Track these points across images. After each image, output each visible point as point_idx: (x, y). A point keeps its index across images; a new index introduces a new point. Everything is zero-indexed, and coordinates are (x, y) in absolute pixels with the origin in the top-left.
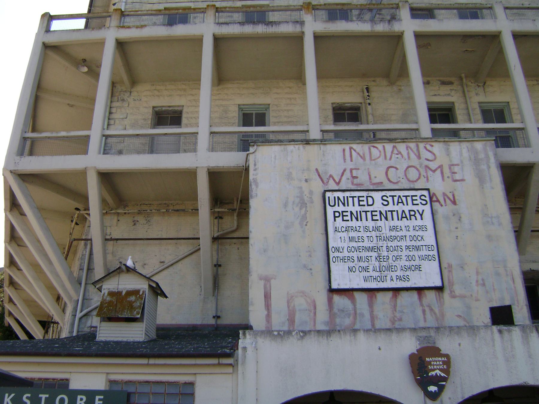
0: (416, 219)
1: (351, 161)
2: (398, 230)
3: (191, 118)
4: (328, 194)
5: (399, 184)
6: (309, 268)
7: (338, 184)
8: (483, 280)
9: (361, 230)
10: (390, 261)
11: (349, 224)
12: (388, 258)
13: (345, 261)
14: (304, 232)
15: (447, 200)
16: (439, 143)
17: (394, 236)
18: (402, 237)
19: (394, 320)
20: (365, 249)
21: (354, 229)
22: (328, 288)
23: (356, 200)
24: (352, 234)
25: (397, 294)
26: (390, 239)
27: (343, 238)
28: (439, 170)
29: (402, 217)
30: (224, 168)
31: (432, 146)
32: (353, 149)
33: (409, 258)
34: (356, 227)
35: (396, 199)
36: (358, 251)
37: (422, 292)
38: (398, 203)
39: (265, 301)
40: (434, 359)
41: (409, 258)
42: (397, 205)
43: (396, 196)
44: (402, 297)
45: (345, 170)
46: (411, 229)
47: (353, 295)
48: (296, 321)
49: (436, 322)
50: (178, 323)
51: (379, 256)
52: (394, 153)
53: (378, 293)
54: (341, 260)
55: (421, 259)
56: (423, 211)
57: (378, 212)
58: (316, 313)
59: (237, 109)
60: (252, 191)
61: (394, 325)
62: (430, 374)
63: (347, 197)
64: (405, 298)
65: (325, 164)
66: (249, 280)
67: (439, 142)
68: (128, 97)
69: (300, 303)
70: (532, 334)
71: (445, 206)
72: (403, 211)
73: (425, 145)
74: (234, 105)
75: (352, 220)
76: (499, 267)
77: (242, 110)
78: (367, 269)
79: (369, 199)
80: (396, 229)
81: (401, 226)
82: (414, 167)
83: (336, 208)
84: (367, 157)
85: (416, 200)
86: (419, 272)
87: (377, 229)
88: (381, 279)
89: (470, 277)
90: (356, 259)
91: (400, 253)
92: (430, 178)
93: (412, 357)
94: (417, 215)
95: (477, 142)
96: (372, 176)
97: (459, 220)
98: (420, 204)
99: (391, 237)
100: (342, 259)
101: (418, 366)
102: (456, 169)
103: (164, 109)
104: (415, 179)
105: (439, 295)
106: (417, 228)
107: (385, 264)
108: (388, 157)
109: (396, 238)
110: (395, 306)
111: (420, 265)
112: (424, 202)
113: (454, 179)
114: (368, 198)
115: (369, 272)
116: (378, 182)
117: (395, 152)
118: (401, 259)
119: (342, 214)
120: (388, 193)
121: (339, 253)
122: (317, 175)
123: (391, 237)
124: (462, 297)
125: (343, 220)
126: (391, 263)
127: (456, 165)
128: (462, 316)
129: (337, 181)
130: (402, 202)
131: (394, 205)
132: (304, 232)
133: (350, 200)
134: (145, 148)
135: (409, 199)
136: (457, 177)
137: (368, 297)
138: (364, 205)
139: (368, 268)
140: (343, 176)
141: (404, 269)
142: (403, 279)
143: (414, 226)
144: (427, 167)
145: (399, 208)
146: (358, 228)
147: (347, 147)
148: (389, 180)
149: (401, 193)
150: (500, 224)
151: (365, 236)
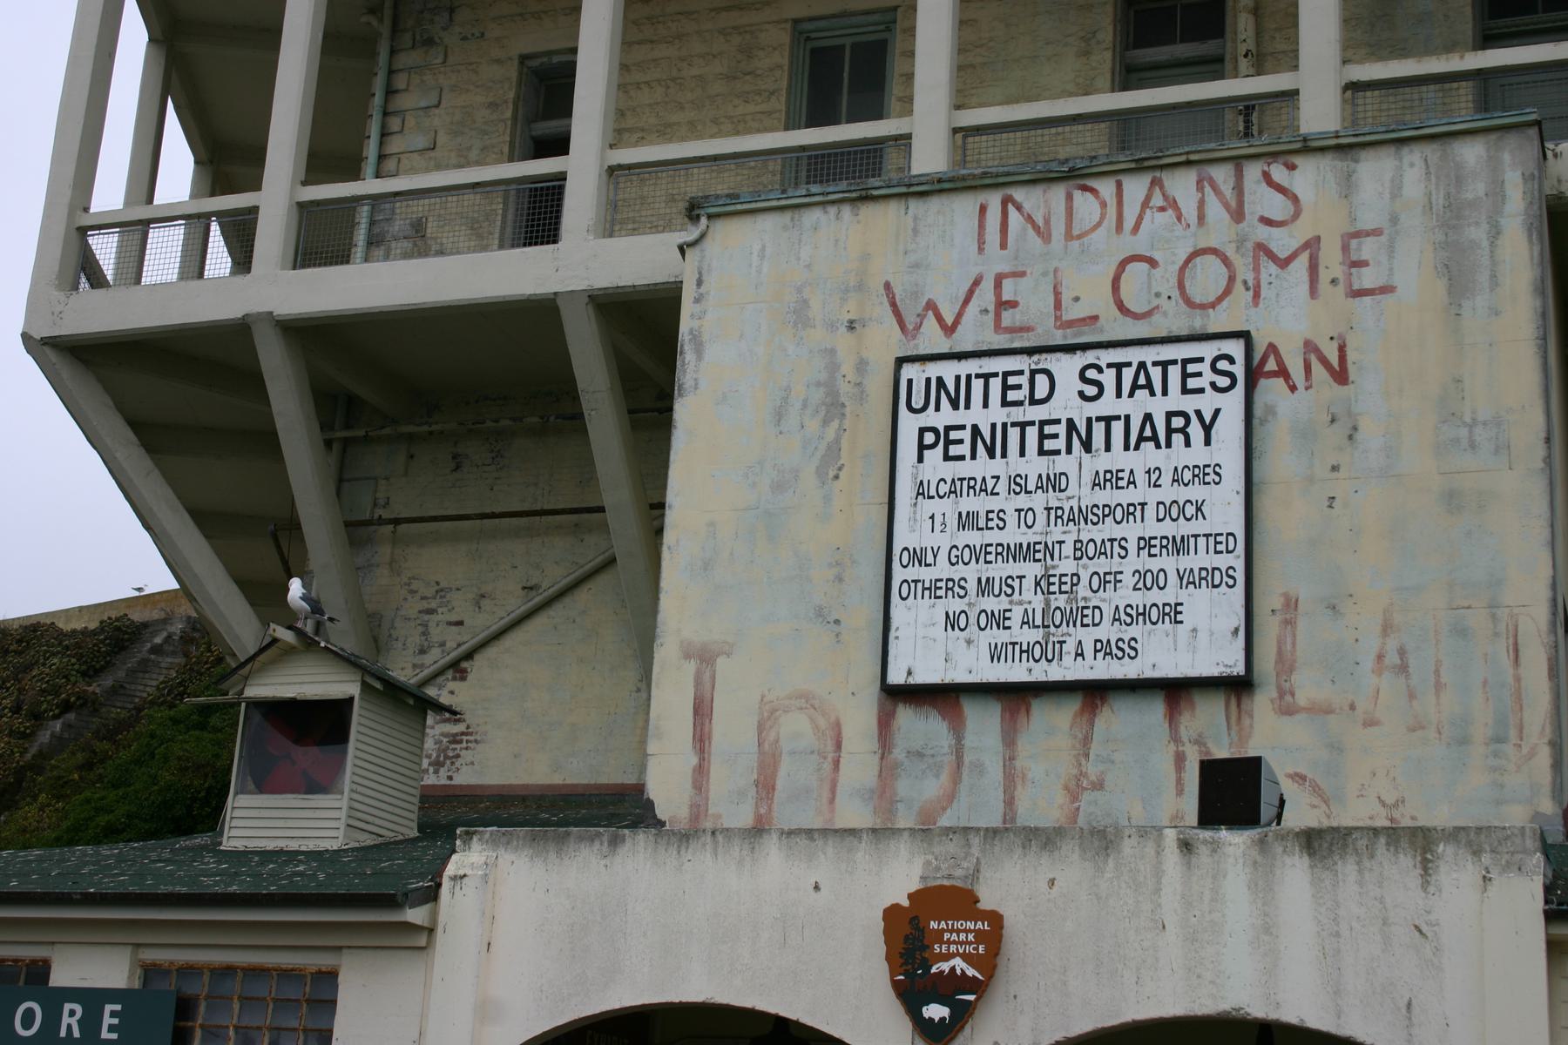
0: (1188, 444)
1: (1003, 246)
2: (1121, 483)
3: (638, 86)
5: (1156, 318)
6: (831, 619)
7: (949, 330)
8: (1402, 652)
9: (1002, 487)
10: (1082, 590)
11: (965, 469)
13: (939, 593)
14: (827, 499)
15: (1317, 367)
16: (1319, 155)
17: (1104, 506)
19: (1078, 785)
20: (1005, 554)
21: (978, 488)
24: (969, 503)
25: (1099, 703)
26: (1090, 517)
27: (939, 519)
28: (1304, 259)
29: (1141, 439)
30: (637, 289)
31: (1292, 167)
34: (984, 479)
35: (1128, 374)
38: (1135, 387)
40: (953, 925)
42: (1131, 395)
43: (1129, 364)
44: (1112, 711)
45: (977, 283)
46: (1166, 479)
48: (779, 784)
50: (569, 781)
53: (1036, 696)
54: (927, 593)
56: (1217, 412)
57: (1064, 422)
58: (838, 761)
59: (785, 38)
60: (685, 371)
62: (934, 970)
63: (969, 377)
64: (1118, 719)
65: (917, 265)
66: (655, 661)
68: (444, 29)
69: (796, 728)
70: (1288, 860)
71: (1307, 389)
72: (1148, 417)
74: (778, 22)
75: (973, 457)
77: (808, 39)
78: (1005, 619)
80: (1114, 480)
81: (1132, 471)
83: (931, 418)
85: (1199, 374)
87: (1053, 483)
88: (1044, 652)
89: (1357, 640)
90: (972, 586)
92: (1264, 293)
93: (892, 913)
94: (1196, 430)
97: (1350, 437)
98: (1208, 389)
99: (1095, 510)
100: (930, 589)
101: (905, 943)
102: (1367, 249)
103: (556, 59)
104: (1212, 299)
105: (1239, 705)
106: (1188, 475)
107: (1060, 601)
108: (1129, 223)
109: (1112, 512)
110: (1087, 741)
111: (1181, 604)
112: (1223, 382)
113: (1356, 287)
115: (1009, 628)
116: (1082, 315)
117: (1158, 200)
118: (1118, 585)
119: (945, 437)
120: (1106, 357)
122: (886, 304)
123: (1095, 510)
124: (1321, 710)
125: (947, 458)
126: (1085, 599)
127: (1368, 234)
128: (1310, 776)
129: (949, 321)
130: (1149, 386)
131: (1119, 395)
132: (827, 499)
133: (978, 385)
134: (494, 207)
135: (1174, 373)
136: (1367, 278)
138: (1019, 403)
139: (1007, 614)
141: (1123, 617)
142: (1115, 651)
143: (1176, 469)
144: (1262, 249)
146: (990, 483)
147: (994, 200)
148: (1121, 307)
149: (1149, 354)
150: (1502, 448)
151: (1010, 510)
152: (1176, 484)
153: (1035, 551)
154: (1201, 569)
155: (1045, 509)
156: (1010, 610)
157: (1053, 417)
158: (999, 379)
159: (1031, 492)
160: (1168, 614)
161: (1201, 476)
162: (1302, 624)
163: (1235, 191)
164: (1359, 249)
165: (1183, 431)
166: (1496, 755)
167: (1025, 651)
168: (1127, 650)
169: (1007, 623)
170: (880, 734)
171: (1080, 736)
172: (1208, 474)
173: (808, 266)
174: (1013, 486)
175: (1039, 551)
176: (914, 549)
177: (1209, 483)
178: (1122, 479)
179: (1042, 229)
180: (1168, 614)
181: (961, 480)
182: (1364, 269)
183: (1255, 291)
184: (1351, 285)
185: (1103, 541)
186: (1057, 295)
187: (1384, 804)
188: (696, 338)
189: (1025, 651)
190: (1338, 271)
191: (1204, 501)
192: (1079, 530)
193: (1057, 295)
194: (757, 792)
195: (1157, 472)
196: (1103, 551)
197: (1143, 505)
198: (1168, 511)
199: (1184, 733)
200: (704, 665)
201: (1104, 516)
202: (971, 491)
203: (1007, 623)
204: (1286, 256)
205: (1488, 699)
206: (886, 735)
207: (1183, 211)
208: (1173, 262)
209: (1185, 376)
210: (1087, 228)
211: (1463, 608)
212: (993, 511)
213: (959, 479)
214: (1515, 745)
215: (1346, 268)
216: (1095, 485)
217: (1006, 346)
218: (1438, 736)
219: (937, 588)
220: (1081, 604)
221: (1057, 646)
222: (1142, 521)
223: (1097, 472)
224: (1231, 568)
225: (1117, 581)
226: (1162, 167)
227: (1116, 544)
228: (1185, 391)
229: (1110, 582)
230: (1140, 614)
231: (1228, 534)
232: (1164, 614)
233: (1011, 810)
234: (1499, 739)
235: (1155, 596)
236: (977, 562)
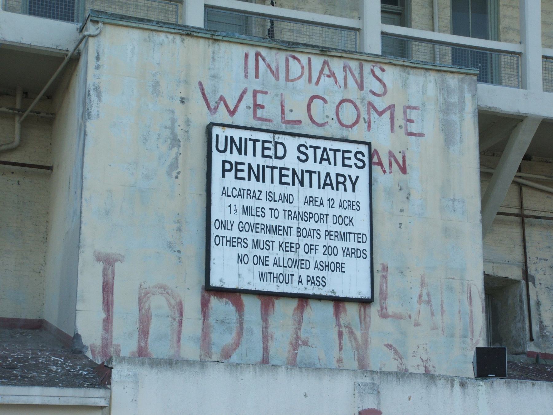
0: (345, 190)
1: (257, 76)
2: (317, 203)
4: (216, 131)
5: (327, 127)
6: (176, 249)
7: (232, 113)
8: (428, 295)
9: (263, 196)
10: (301, 251)
11: (245, 184)
12: (298, 247)
13: (234, 244)
15: (394, 164)
16: (394, 67)
17: (310, 213)
18: (322, 216)
19: (297, 343)
21: (252, 195)
23: (259, 145)
25: (305, 304)
26: (304, 217)
27: (233, 208)
28: (388, 114)
29: (325, 184)
30: (32, 47)
31: (383, 70)
32: (261, 56)
33: (330, 251)
34: (254, 191)
35: (319, 152)
37: (341, 304)
38: (322, 159)
39: (103, 296)
41: (330, 251)
42: (321, 162)
43: (319, 148)
45: (244, 92)
46: (337, 205)
47: (240, 300)
48: (151, 331)
49: (356, 352)
51: (286, 243)
52: (324, 73)
53: (277, 299)
54: (228, 243)
56: (358, 177)
58: (181, 322)
61: (296, 352)
63: (246, 139)
65: (214, 77)
67: (395, 65)
71: (390, 173)
72: (328, 175)
73: (374, 67)
76: (453, 279)
78: (266, 261)
79: (280, 147)
80: (314, 201)
81: (322, 199)
82: (351, 102)
84: (282, 75)
85: (350, 158)
86: (341, 273)
87: (287, 198)
88: (284, 278)
89: (411, 288)
90: (250, 243)
91: (315, 241)
94: (348, 184)
95: (451, 75)
97: (408, 198)
98: (354, 166)
99: (306, 214)
100: (230, 241)
102: (413, 115)
104: (350, 123)
105: (365, 312)
106: (346, 205)
108: (314, 79)
110: (300, 322)
111: (344, 264)
112: (360, 164)
113: (409, 131)
115: (268, 265)
117: (326, 71)
118: (317, 251)
119: (236, 167)
123: (306, 214)
124: (398, 317)
125: (236, 178)
126: (302, 255)
127: (413, 108)
128: (394, 346)
129: (232, 108)
130: (328, 159)
131: (315, 162)
135: (339, 155)
136: (413, 128)
137: (262, 304)
138: (270, 157)
139: (267, 259)
141: (319, 266)
142: (316, 282)
144: (370, 104)
145: (323, 168)
146: (258, 194)
147: (252, 52)
151: (267, 209)
152: (341, 208)
153: (279, 230)
154: (352, 249)
155: (283, 210)
156: (268, 257)
157: (286, 166)
159: (276, 201)
160: (338, 267)
162: (390, 278)
163: (360, 75)
164: (410, 114)
165: (343, 183)
166: (464, 342)
167: (275, 277)
168: (321, 282)
169: (267, 263)
170: (203, 310)
171: (297, 319)
172: (354, 205)
173: (159, 64)
175: (281, 230)
177: (355, 210)
178: (317, 201)
179: (275, 73)
180: (338, 267)
181: (244, 190)
183: (368, 124)
184: (407, 130)
185: (310, 230)
186: (282, 106)
187: (422, 360)
188: (97, 89)
191: (353, 217)
192: (299, 223)
193: (282, 106)
194: (139, 334)
195: (333, 200)
197: (327, 215)
198: (338, 220)
199: (342, 322)
200: (108, 266)
201: (310, 218)
202: (249, 196)
203: (267, 263)
204: (381, 111)
205: (461, 319)
206: (205, 311)
207: (337, 79)
208: (334, 103)
209: (344, 158)
210: (295, 77)
211: (451, 279)
212: (259, 208)
213: (242, 189)
214: (471, 339)
215: (405, 121)
216: (305, 202)
217: (259, 127)
218: (442, 333)
219: (233, 242)
220: (301, 258)
221: (290, 277)
222: (327, 223)
223: (306, 197)
225: (316, 249)
226: (328, 56)
227: (315, 232)
228: (344, 165)
229: (313, 249)
230: (327, 266)
232: (337, 267)
233: (267, 352)
234: (465, 336)
235: (332, 258)
236: (252, 231)
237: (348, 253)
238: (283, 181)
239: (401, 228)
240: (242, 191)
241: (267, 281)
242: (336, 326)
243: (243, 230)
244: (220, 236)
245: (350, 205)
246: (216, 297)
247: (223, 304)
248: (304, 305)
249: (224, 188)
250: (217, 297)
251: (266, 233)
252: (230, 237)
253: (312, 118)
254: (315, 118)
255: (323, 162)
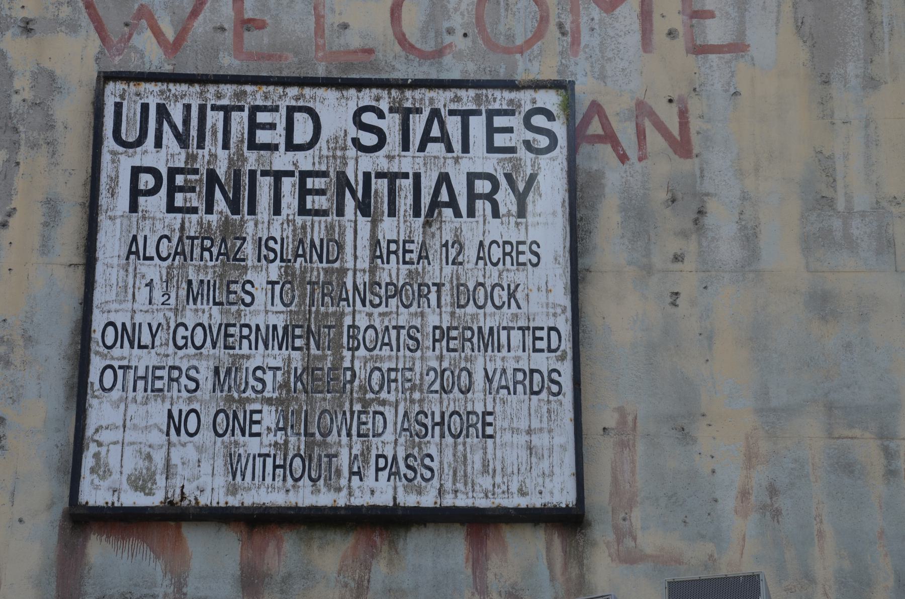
0: (496, 214)
5: (448, 59)
13: (159, 384)
21: (215, 251)
22: (65, 503)
35: (418, 125)
36: (221, 343)
38: (426, 139)
42: (422, 148)
43: (419, 111)
54: (141, 384)
55: (495, 385)
63: (202, 109)
71: (640, 159)
72: (444, 179)
78: (253, 422)
83: (148, 156)
85: (510, 130)
89: (713, 472)
92: (585, 38)
94: (506, 199)
96: (332, 20)
100: (145, 378)
104: (519, 41)
106: (496, 253)
111: (490, 414)
114: (297, 115)
115: (258, 435)
121: (136, 351)
125: (171, 208)
129: (170, 34)
130: (445, 138)
131: (406, 147)
135: (477, 125)
139: (256, 417)
140: (201, 18)
142: (403, 469)
148: (402, 40)
156: (260, 412)
158: (245, 114)
161: (514, 254)
165: (490, 197)
167: (279, 467)
169: (256, 428)
172: (523, 253)
174: (264, 251)
176: (124, 325)
177: (524, 264)
182: (708, 22)
183: (573, 37)
184: (693, 40)
186: (319, 18)
189: (279, 467)
190: (677, 22)
193: (319, 18)
196: (386, 340)
197: (439, 286)
203: (256, 428)
209: (491, 130)
215: (685, 18)
224: (554, 370)
227: (403, 332)
228: (491, 148)
230: (437, 424)
231: (551, 329)
237: (503, 383)
238: (309, 206)
239: (676, 306)
240: (187, 242)
241: (253, 479)
242: (473, 594)
243: (186, 345)
244: (117, 367)
245: (509, 254)
246: (105, 536)
247: (125, 554)
248: (375, 542)
249: (135, 238)
250: (108, 537)
251: (256, 348)
252: (147, 367)
253: (406, 40)
254: (412, 40)
255: (431, 146)
